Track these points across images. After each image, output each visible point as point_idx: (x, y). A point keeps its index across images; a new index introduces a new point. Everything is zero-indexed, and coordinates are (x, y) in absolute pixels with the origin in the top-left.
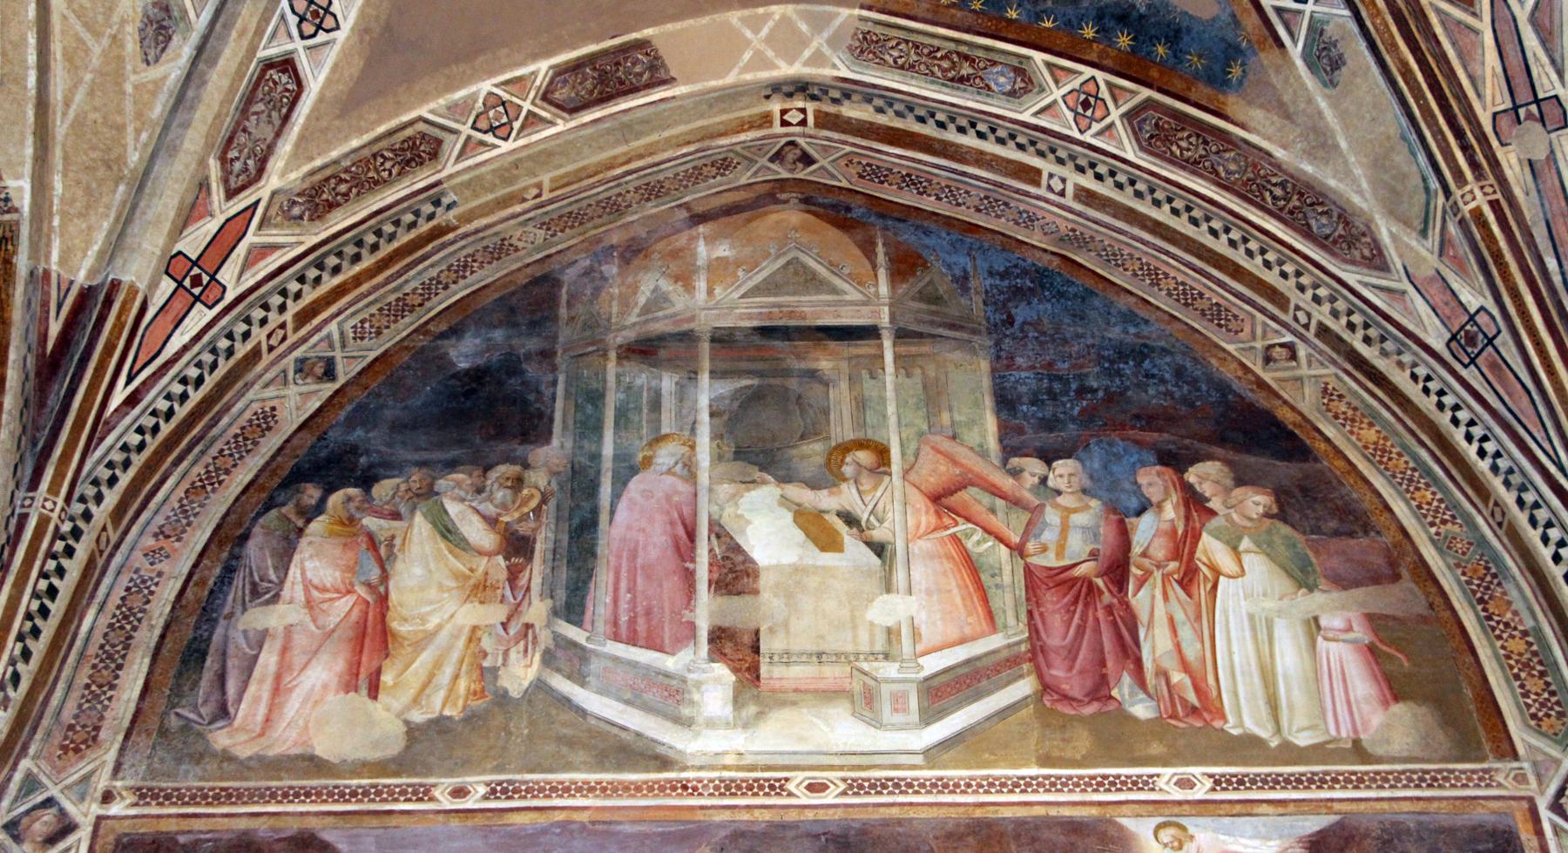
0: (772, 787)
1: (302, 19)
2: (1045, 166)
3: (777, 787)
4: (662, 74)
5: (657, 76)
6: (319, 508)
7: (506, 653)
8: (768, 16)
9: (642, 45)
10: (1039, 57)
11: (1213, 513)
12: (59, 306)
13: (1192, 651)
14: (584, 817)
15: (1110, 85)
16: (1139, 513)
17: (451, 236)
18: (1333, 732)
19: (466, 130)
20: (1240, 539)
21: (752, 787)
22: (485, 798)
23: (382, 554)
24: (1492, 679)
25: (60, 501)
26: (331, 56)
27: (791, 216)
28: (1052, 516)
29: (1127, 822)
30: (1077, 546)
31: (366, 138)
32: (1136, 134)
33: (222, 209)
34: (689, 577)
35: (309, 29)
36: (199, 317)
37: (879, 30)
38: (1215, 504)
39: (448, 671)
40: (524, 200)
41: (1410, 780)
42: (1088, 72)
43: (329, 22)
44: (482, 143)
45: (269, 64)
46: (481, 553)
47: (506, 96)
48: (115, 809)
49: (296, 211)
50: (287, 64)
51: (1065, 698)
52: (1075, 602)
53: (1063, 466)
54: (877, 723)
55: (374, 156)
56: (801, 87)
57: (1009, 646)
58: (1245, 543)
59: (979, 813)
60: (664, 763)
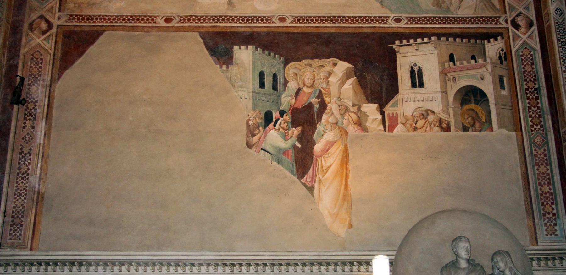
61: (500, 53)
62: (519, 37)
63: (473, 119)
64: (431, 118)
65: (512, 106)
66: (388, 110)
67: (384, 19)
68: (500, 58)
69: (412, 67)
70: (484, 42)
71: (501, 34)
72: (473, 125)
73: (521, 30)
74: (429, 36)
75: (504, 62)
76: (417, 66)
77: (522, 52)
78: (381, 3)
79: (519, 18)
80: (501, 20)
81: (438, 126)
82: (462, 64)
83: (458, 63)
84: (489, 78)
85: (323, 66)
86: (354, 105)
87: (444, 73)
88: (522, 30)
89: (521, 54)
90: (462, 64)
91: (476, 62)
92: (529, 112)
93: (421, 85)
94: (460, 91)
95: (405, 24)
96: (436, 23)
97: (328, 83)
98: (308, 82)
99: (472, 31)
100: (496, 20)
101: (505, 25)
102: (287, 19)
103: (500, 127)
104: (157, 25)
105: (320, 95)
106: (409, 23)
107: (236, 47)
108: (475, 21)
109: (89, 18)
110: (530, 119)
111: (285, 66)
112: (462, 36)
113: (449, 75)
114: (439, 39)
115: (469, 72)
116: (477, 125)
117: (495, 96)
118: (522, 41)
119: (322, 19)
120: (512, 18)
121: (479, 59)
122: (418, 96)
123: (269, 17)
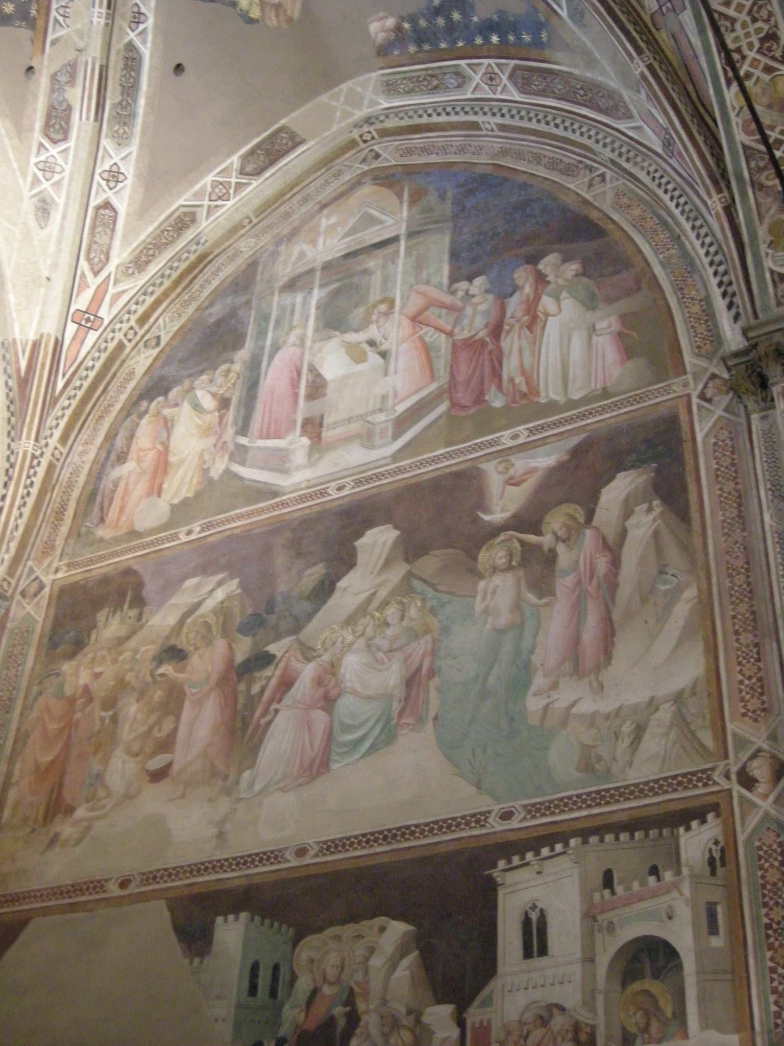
0: (321, 494)
1: (108, 181)
2: (479, 119)
3: (323, 493)
4: (298, 140)
5: (296, 142)
6: (146, 412)
7: (214, 459)
8: (341, 90)
9: (282, 129)
10: (462, 63)
11: (549, 283)
12: (24, 352)
13: (527, 363)
14: (237, 531)
15: (498, 65)
16: (511, 295)
17: (211, 257)
18: (593, 387)
19: (206, 203)
20: (560, 293)
21: (311, 496)
22: (200, 532)
23: (168, 425)
24: (680, 331)
25: (32, 442)
26: (126, 193)
27: (367, 190)
28: (469, 311)
29: (483, 466)
30: (479, 322)
31: (156, 224)
32: (516, 85)
33: (94, 282)
34: (296, 396)
35: (112, 184)
36: (92, 336)
37: (391, 78)
38: (551, 278)
39: (189, 475)
40: (244, 227)
41: (628, 402)
42: (486, 61)
43: (121, 177)
44: (217, 206)
45: (98, 208)
46: (208, 412)
47: (221, 180)
48: (60, 575)
49: (130, 271)
50: (107, 205)
51: (463, 407)
52: (474, 354)
53: (479, 281)
54: (372, 447)
55: (162, 232)
56: (368, 121)
57: (438, 388)
58: (564, 294)
59: (413, 481)
60: (275, 494)
61: (710, 851)
62: (754, 805)
63: (647, 1014)
64: (558, 1022)
65: (733, 971)
66: (474, 1015)
67: (479, 819)
68: (711, 862)
69: (526, 913)
70: (678, 831)
71: (715, 808)
72: (646, 1029)
73: (760, 790)
74: (564, 838)
75: (720, 871)
76: (537, 910)
77: (760, 840)
78: (478, 786)
79: (755, 764)
80: (716, 776)
81: (570, 1040)
82: (628, 889)
83: (619, 889)
84: (684, 913)
85: (360, 937)
86: (409, 1012)
87: (590, 916)
88: (761, 788)
89: (757, 844)
90: (628, 889)
91: (659, 880)
92: (772, 980)
93: (543, 951)
94: (621, 951)
95: (520, 821)
96: (580, 808)
97: (366, 972)
98: (331, 973)
99: (655, 811)
100: (705, 777)
101: (725, 785)
102: (308, 850)
103: (705, 1024)
104: (108, 896)
105: (350, 1000)
106: (528, 817)
107: (219, 920)
108: (632, 793)
109: (16, 898)
110: (772, 998)
111: (295, 943)
112: (632, 826)
113: (599, 918)
114: (585, 842)
115: (643, 905)
116: (654, 1027)
117: (696, 953)
118: (760, 814)
119: (368, 839)
120: (740, 765)
121: (665, 871)
122: (535, 975)
123: (280, 851)
